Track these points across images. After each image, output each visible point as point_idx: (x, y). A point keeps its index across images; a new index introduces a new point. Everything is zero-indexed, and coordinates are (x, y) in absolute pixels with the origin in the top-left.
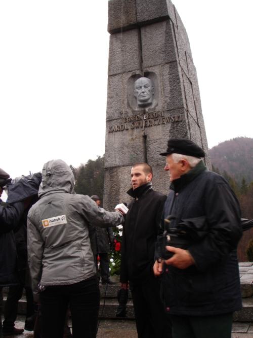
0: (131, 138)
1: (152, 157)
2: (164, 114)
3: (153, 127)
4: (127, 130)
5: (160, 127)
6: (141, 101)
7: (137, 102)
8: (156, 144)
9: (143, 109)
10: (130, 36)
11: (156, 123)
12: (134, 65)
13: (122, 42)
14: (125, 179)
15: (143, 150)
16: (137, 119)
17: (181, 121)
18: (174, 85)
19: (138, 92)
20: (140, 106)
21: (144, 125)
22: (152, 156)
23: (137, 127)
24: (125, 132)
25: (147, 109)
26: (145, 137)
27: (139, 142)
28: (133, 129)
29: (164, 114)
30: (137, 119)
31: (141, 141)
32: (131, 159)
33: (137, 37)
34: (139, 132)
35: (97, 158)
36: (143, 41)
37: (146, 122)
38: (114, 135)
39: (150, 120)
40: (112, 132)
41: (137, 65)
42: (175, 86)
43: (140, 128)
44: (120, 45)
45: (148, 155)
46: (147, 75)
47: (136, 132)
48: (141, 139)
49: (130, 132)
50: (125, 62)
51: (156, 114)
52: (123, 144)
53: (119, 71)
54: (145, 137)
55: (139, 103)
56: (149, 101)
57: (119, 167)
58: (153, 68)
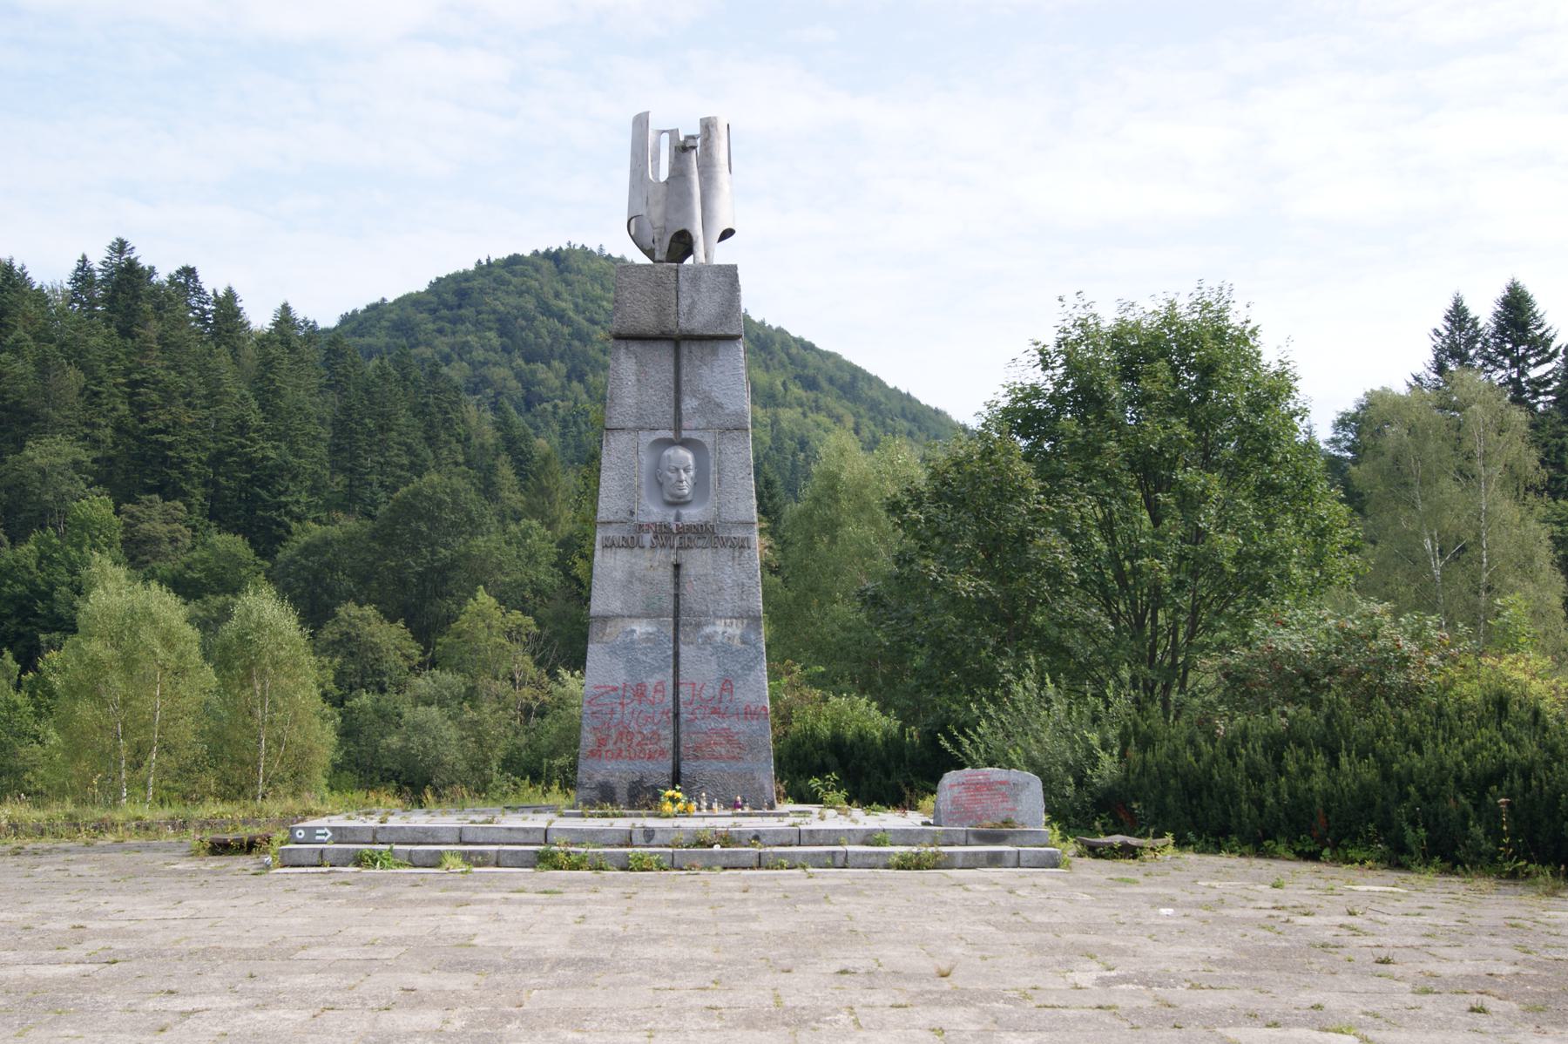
3: (695, 551)
5: (709, 552)
11: (700, 543)
13: (640, 363)
21: (676, 544)
23: (663, 546)
26: (677, 567)
27: (665, 576)
33: (672, 359)
36: (684, 371)
46: (686, 443)
47: (660, 555)
48: (670, 569)
49: (648, 554)
52: (632, 574)
53: (631, 425)
54: (677, 567)
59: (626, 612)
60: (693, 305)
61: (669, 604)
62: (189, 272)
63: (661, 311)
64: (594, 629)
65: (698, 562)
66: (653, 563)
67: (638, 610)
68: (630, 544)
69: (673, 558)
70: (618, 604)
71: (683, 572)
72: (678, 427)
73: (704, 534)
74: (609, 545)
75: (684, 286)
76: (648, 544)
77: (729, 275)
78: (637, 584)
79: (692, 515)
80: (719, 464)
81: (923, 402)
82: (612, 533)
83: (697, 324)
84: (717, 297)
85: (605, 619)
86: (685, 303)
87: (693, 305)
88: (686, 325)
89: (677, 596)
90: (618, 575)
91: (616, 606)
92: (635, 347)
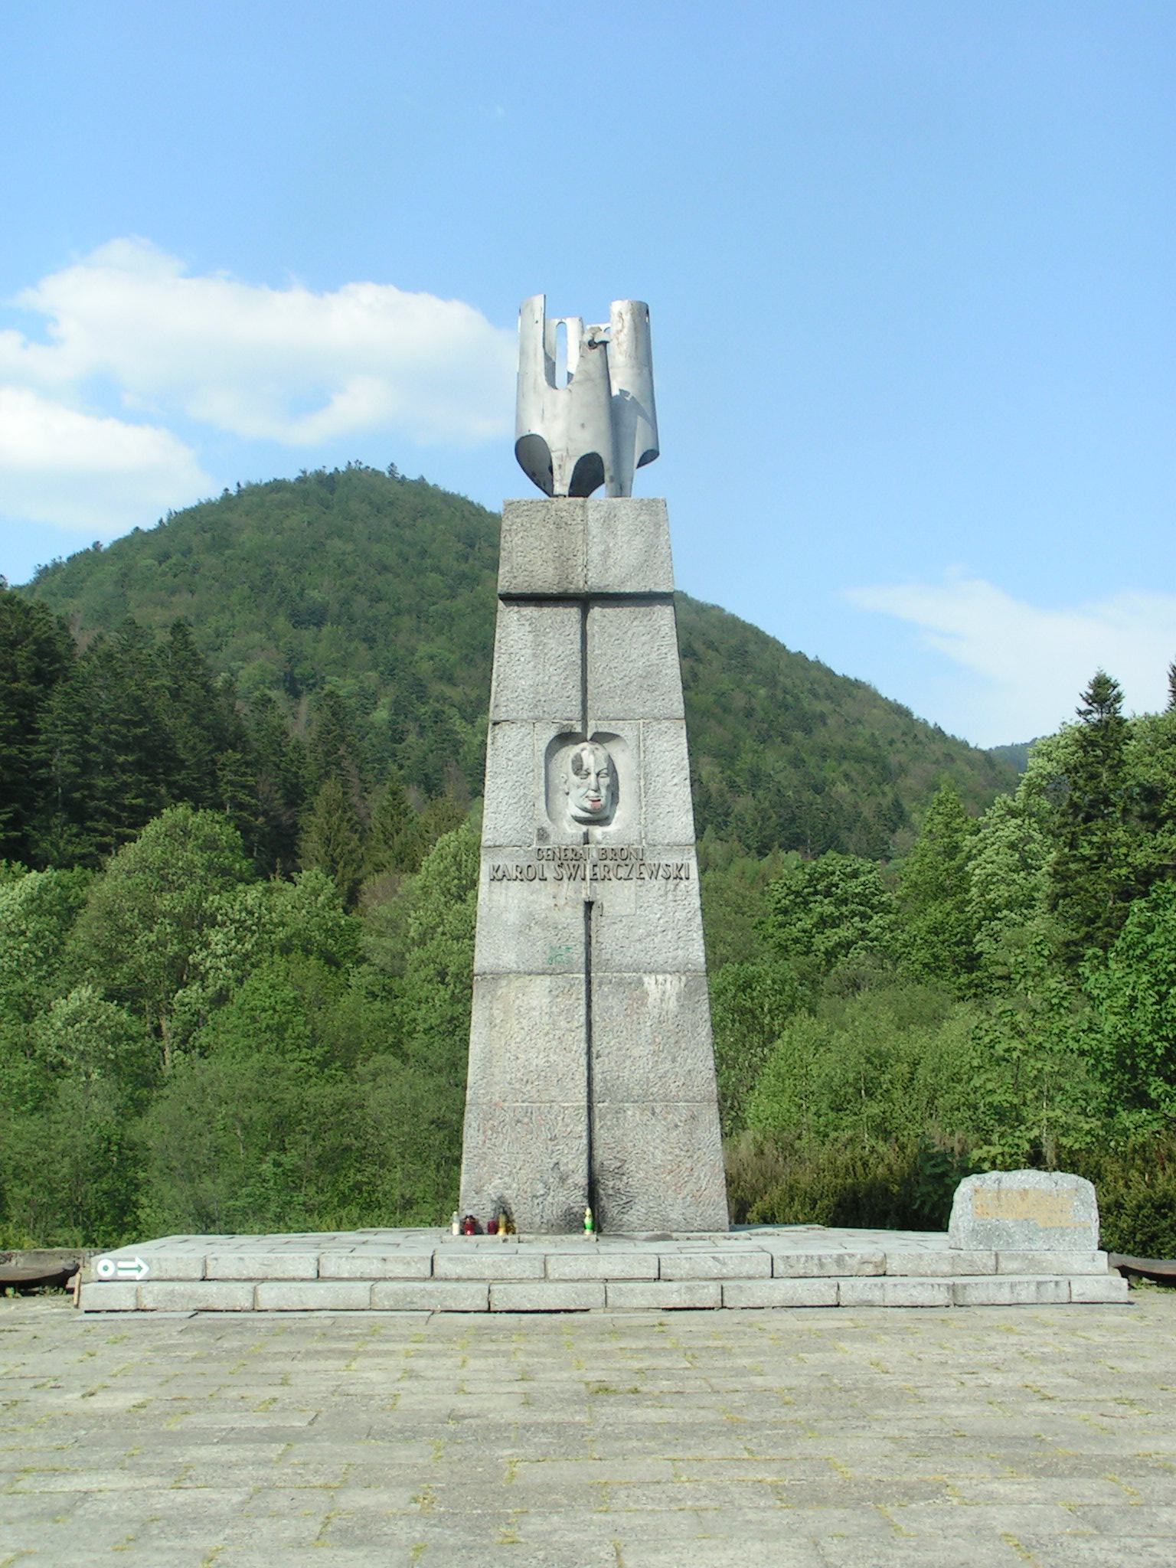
0: (552, 903)
8: (620, 925)
38: (507, 888)
39: (607, 862)
47: (567, 888)
48: (581, 908)
49: (550, 887)
54: (589, 905)
59: (522, 968)
60: (606, 554)
61: (578, 955)
62: (137, 529)
63: (563, 560)
65: (619, 897)
66: (557, 901)
67: (539, 964)
68: (527, 875)
69: (584, 895)
70: (513, 957)
71: (594, 913)
73: (624, 860)
74: (499, 876)
75: (595, 528)
77: (654, 508)
78: (536, 929)
81: (839, 672)
82: (507, 861)
83: (612, 581)
84: (638, 542)
85: (497, 976)
86: (595, 552)
87: (606, 554)
88: (596, 580)
89: (588, 944)
90: (512, 917)
91: (509, 959)
92: (530, 611)
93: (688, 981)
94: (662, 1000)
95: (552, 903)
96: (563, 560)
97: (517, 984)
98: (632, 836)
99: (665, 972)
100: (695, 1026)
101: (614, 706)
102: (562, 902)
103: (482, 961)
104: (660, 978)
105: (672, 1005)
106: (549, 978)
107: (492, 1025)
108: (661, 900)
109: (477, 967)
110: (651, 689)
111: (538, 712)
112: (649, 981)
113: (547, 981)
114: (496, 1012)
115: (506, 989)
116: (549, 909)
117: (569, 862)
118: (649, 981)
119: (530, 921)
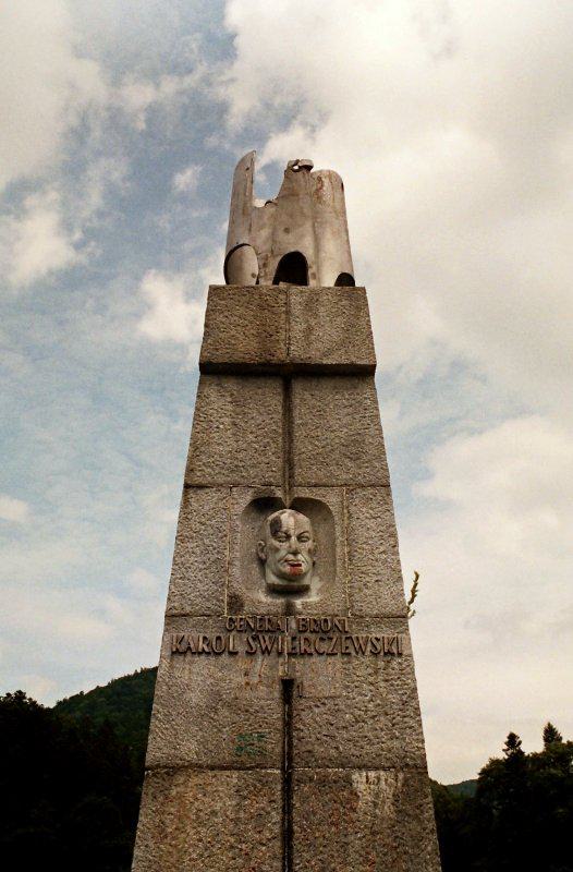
0: (242, 680)
1: (309, 752)
2: (350, 626)
4: (233, 654)
6: (281, 575)
7: (264, 575)
8: (322, 709)
9: (280, 601)
10: (260, 391)
11: (325, 647)
12: (268, 469)
14: (214, 813)
15: (279, 725)
16: (267, 626)
17: (400, 655)
18: (382, 549)
19: (277, 550)
20: (273, 590)
22: (309, 747)
23: (266, 652)
24: (225, 658)
25: (298, 603)
26: (288, 686)
27: (267, 699)
28: (251, 654)
29: (350, 626)
30: (267, 626)
31: (277, 695)
32: (240, 748)
33: (281, 398)
34: (272, 667)
35: (78, 693)
36: (296, 413)
37: (294, 639)
39: (307, 635)
40: (184, 653)
41: (274, 475)
42: (384, 552)
43: (273, 654)
44: (230, 407)
45: (295, 742)
47: (261, 664)
48: (278, 687)
49: (242, 663)
50: (240, 456)
51: (326, 621)
52: (216, 696)
54: (288, 686)
55: (273, 579)
56: (306, 581)
57: (199, 768)
58: (322, 491)
59: (204, 760)
61: (274, 744)
63: (266, 336)
64: (148, 790)
70: (193, 746)
72: (289, 478)
75: (297, 310)
76: (242, 649)
79: (312, 601)
80: (348, 531)
85: (173, 770)
86: (298, 328)
88: (298, 352)
90: (195, 697)
91: (190, 749)
92: (231, 385)
93: (406, 780)
94: (375, 805)
95: (242, 680)
96: (266, 336)
97: (195, 780)
98: (335, 606)
99: (376, 769)
100: (418, 839)
101: (320, 474)
102: (255, 680)
103: (157, 749)
104: (372, 774)
105: (388, 810)
106: (235, 774)
107: (161, 833)
108: (371, 679)
109: (149, 759)
110: (355, 458)
111: (235, 477)
112: (359, 778)
113: (234, 777)
114: (168, 819)
115: (187, 787)
116: (240, 688)
117: (262, 633)
118: (359, 778)
119: (216, 698)
